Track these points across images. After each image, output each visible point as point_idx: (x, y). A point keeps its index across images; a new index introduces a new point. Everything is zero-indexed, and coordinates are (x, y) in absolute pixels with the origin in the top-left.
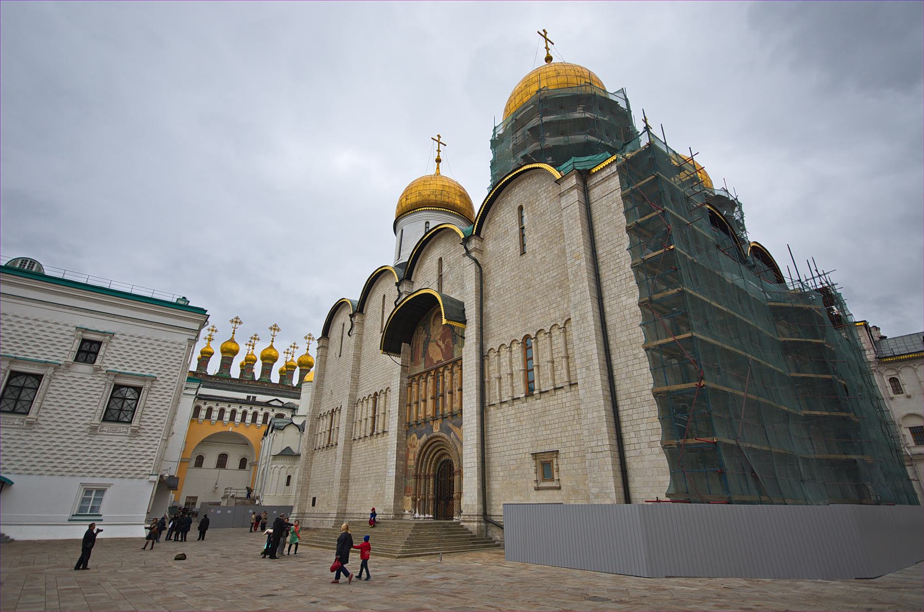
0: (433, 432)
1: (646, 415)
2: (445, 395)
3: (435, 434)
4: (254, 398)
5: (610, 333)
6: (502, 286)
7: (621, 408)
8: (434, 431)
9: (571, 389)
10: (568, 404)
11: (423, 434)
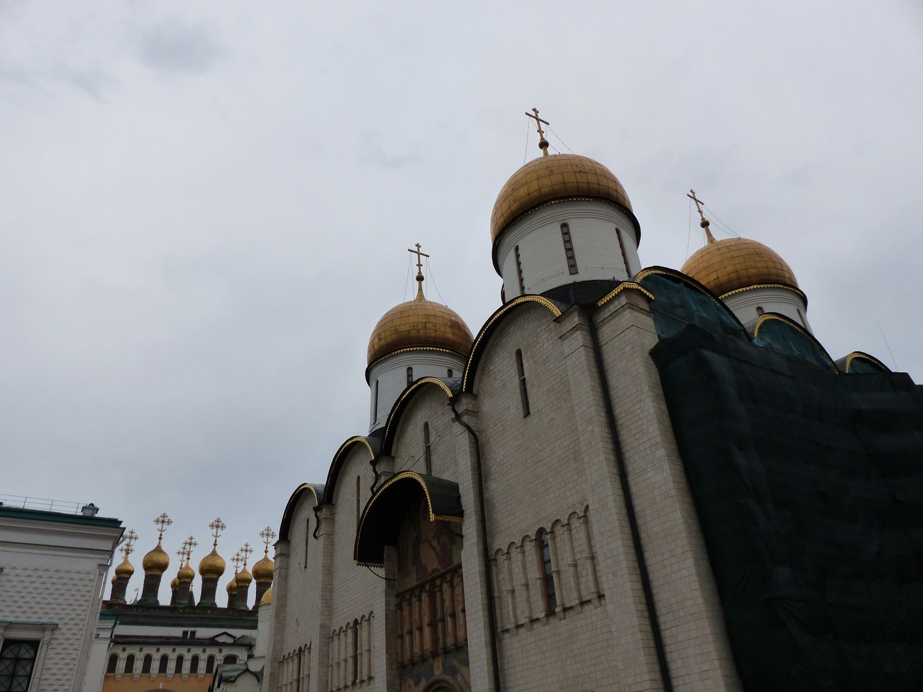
0: (433, 674)
4: (193, 633)
5: (640, 522)
6: (504, 461)
7: (662, 627)
9: (600, 603)
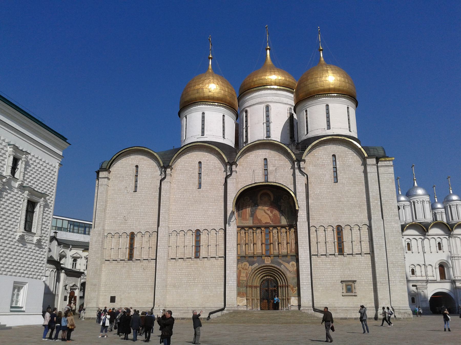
1: (399, 271)
2: (274, 243)
3: (268, 265)
6: (320, 194)
8: (265, 262)
10: (362, 262)
11: (256, 263)
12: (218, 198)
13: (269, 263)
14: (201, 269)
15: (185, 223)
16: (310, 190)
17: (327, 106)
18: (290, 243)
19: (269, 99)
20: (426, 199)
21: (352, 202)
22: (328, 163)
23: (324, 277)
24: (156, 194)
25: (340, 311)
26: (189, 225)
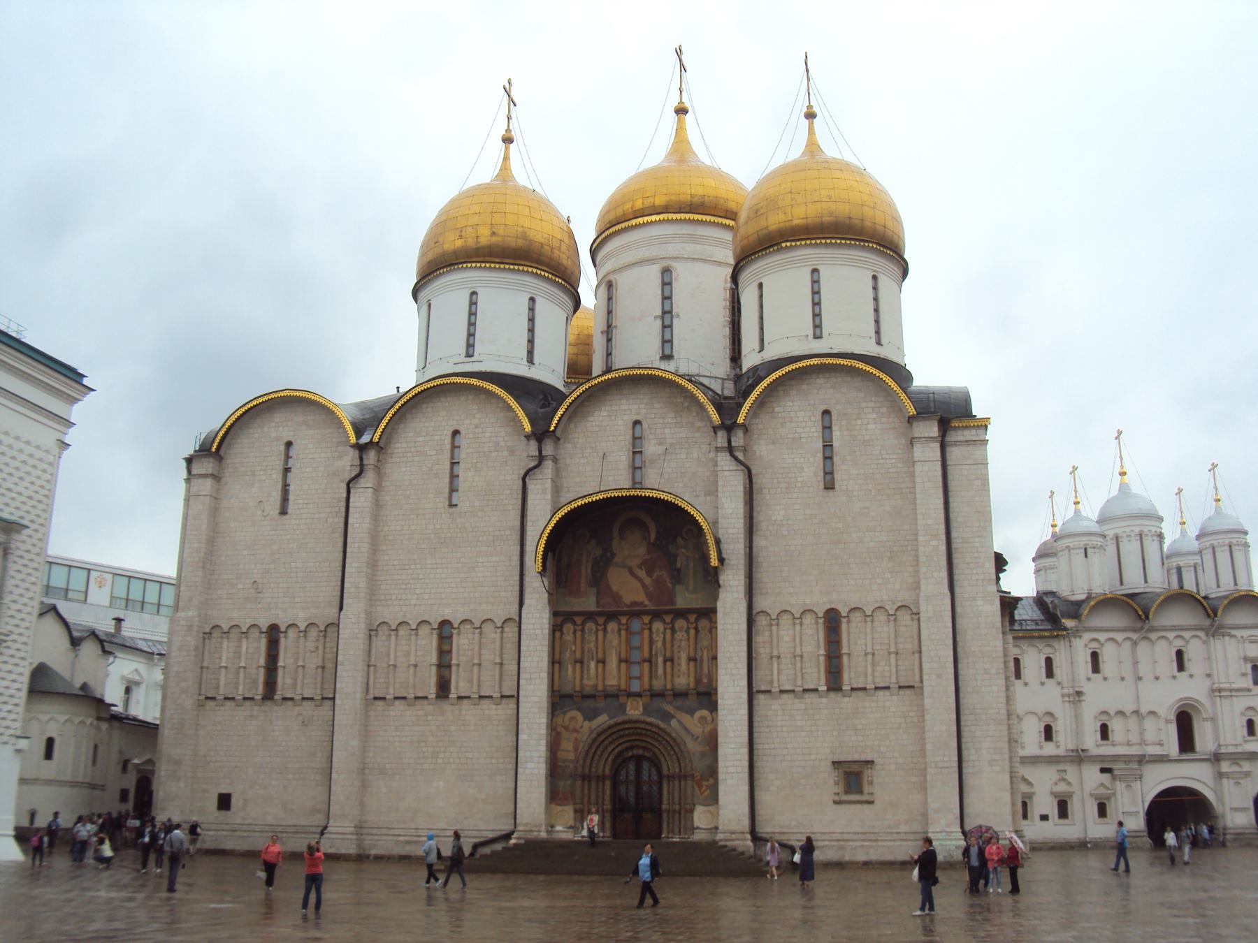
0: (624, 711)
2: (654, 659)
3: (634, 718)
6: (784, 522)
7: (962, 723)
10: (892, 709)
12: (503, 533)
13: (637, 712)
14: (453, 728)
15: (413, 602)
16: (759, 512)
17: (815, 271)
18: (698, 658)
19: (672, 249)
20: (1123, 529)
21: (871, 544)
22: (811, 435)
23: (785, 752)
24: (336, 520)
25: (826, 843)
26: (423, 608)
